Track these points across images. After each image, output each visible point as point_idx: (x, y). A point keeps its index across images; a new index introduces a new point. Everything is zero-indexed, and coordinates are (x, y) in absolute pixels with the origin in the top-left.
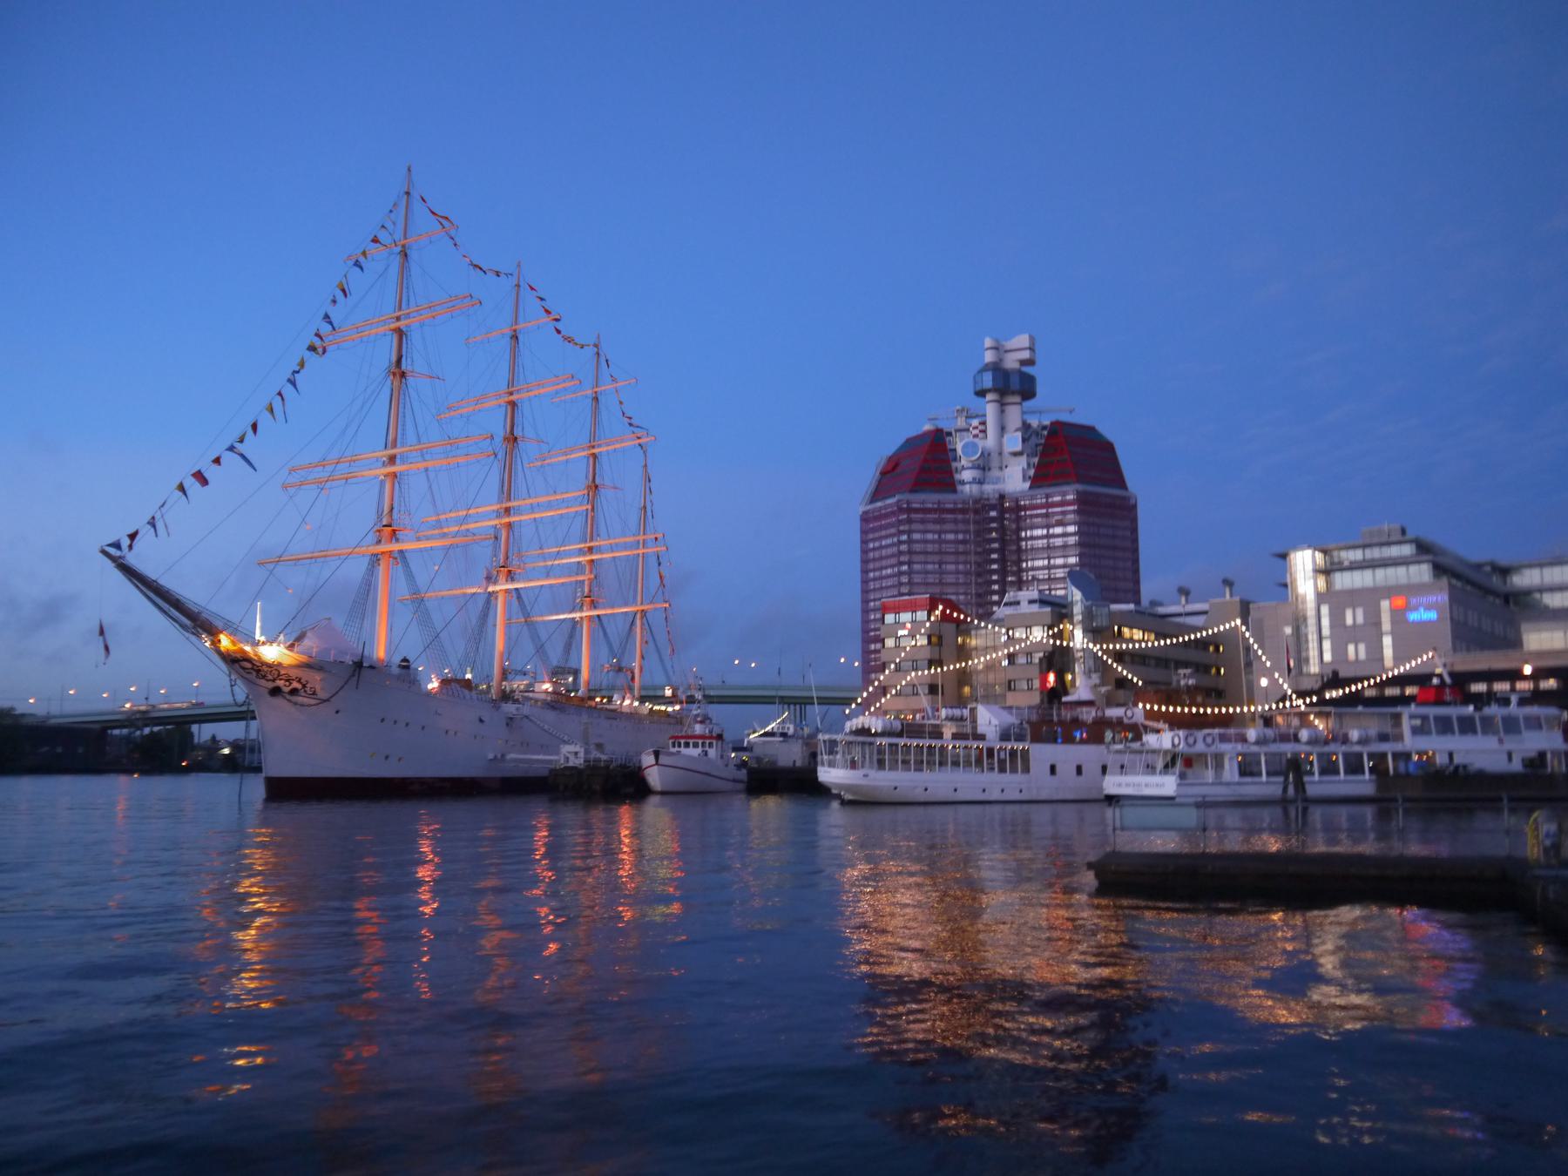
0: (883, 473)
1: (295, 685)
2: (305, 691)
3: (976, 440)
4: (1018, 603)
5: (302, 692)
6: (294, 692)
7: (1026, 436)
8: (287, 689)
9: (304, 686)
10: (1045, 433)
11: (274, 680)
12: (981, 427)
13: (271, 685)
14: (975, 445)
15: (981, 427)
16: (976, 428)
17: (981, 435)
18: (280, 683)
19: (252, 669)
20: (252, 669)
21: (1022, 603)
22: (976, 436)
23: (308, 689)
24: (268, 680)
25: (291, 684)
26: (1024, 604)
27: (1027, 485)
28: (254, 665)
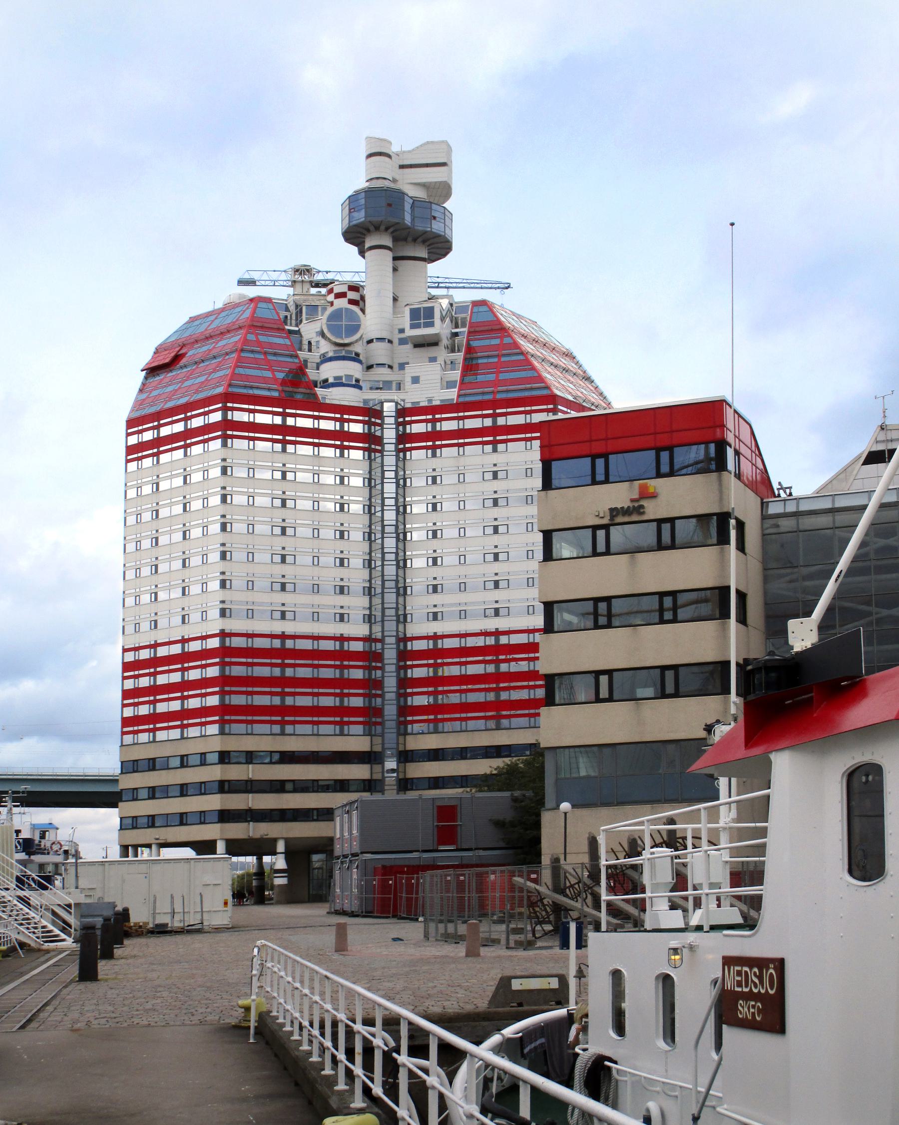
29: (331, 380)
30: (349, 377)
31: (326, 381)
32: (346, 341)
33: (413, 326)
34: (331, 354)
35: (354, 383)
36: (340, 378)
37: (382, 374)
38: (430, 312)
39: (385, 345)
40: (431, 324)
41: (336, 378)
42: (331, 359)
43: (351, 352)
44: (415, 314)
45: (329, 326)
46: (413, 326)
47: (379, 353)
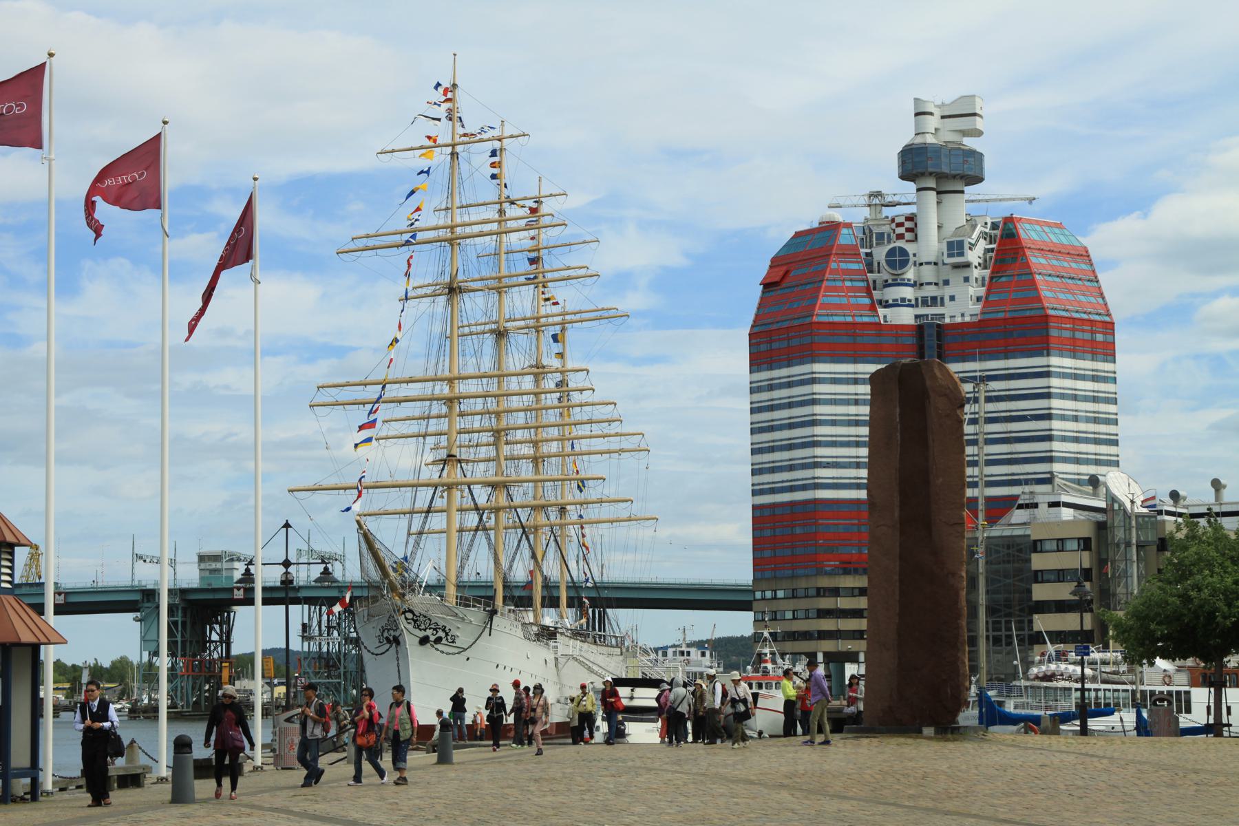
0: (767, 285)
1: (441, 634)
2: (447, 639)
3: (900, 244)
4: (1035, 506)
5: (444, 641)
6: (439, 640)
7: (973, 242)
8: (432, 638)
9: (447, 634)
10: (998, 232)
11: (425, 630)
12: (908, 224)
13: (422, 634)
14: (903, 252)
15: (908, 224)
16: (900, 225)
17: (908, 236)
18: (429, 632)
19: (413, 619)
20: (413, 619)
21: (1040, 506)
22: (900, 237)
23: (449, 637)
24: (420, 630)
25: (437, 632)
26: (1043, 507)
27: (977, 308)
28: (414, 615)
29: (890, 302)
30: (903, 300)
31: (887, 301)
32: (900, 272)
33: (950, 255)
34: (890, 281)
35: (907, 303)
36: (897, 300)
37: (930, 291)
38: (960, 244)
39: (932, 267)
40: (962, 254)
41: (894, 300)
42: (890, 285)
43: (904, 280)
44: (950, 245)
45: (888, 262)
46: (950, 255)
47: (928, 274)
